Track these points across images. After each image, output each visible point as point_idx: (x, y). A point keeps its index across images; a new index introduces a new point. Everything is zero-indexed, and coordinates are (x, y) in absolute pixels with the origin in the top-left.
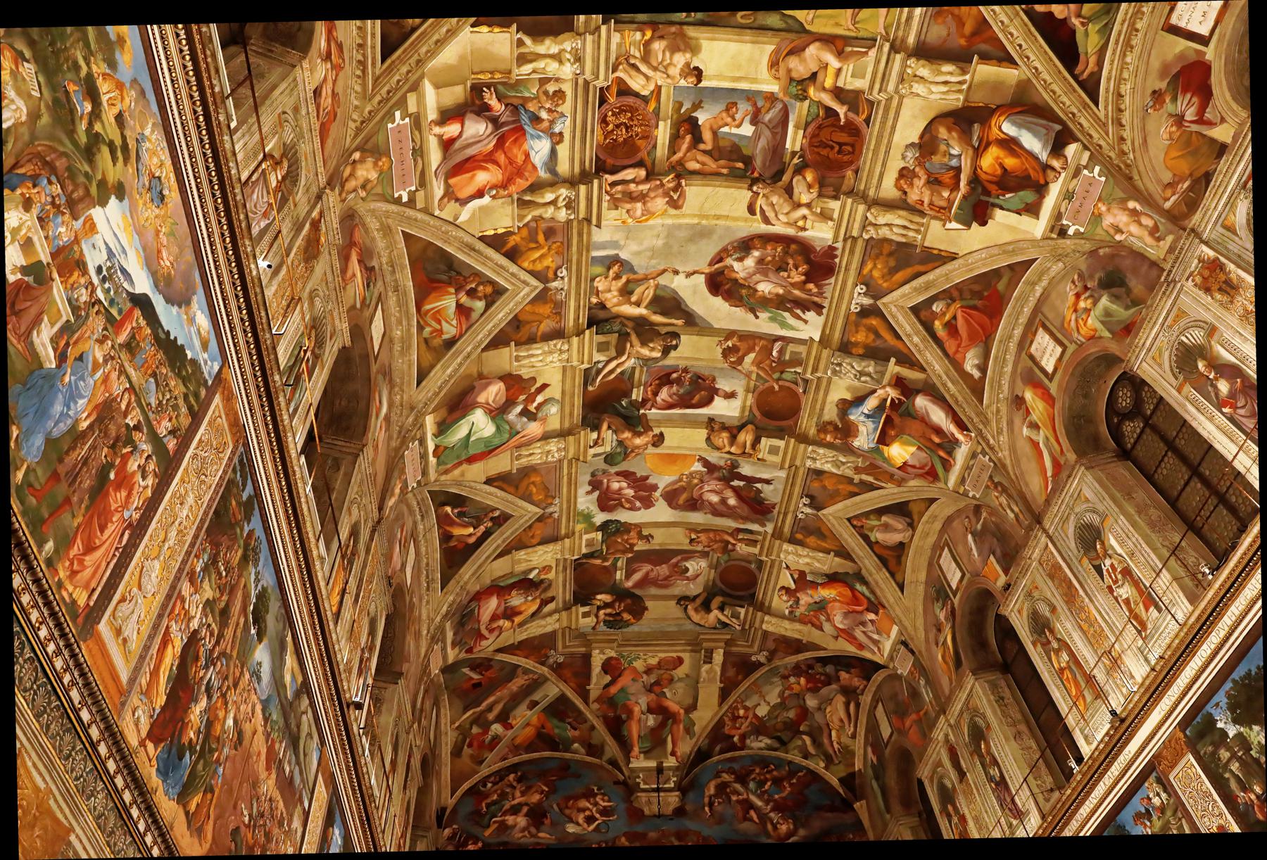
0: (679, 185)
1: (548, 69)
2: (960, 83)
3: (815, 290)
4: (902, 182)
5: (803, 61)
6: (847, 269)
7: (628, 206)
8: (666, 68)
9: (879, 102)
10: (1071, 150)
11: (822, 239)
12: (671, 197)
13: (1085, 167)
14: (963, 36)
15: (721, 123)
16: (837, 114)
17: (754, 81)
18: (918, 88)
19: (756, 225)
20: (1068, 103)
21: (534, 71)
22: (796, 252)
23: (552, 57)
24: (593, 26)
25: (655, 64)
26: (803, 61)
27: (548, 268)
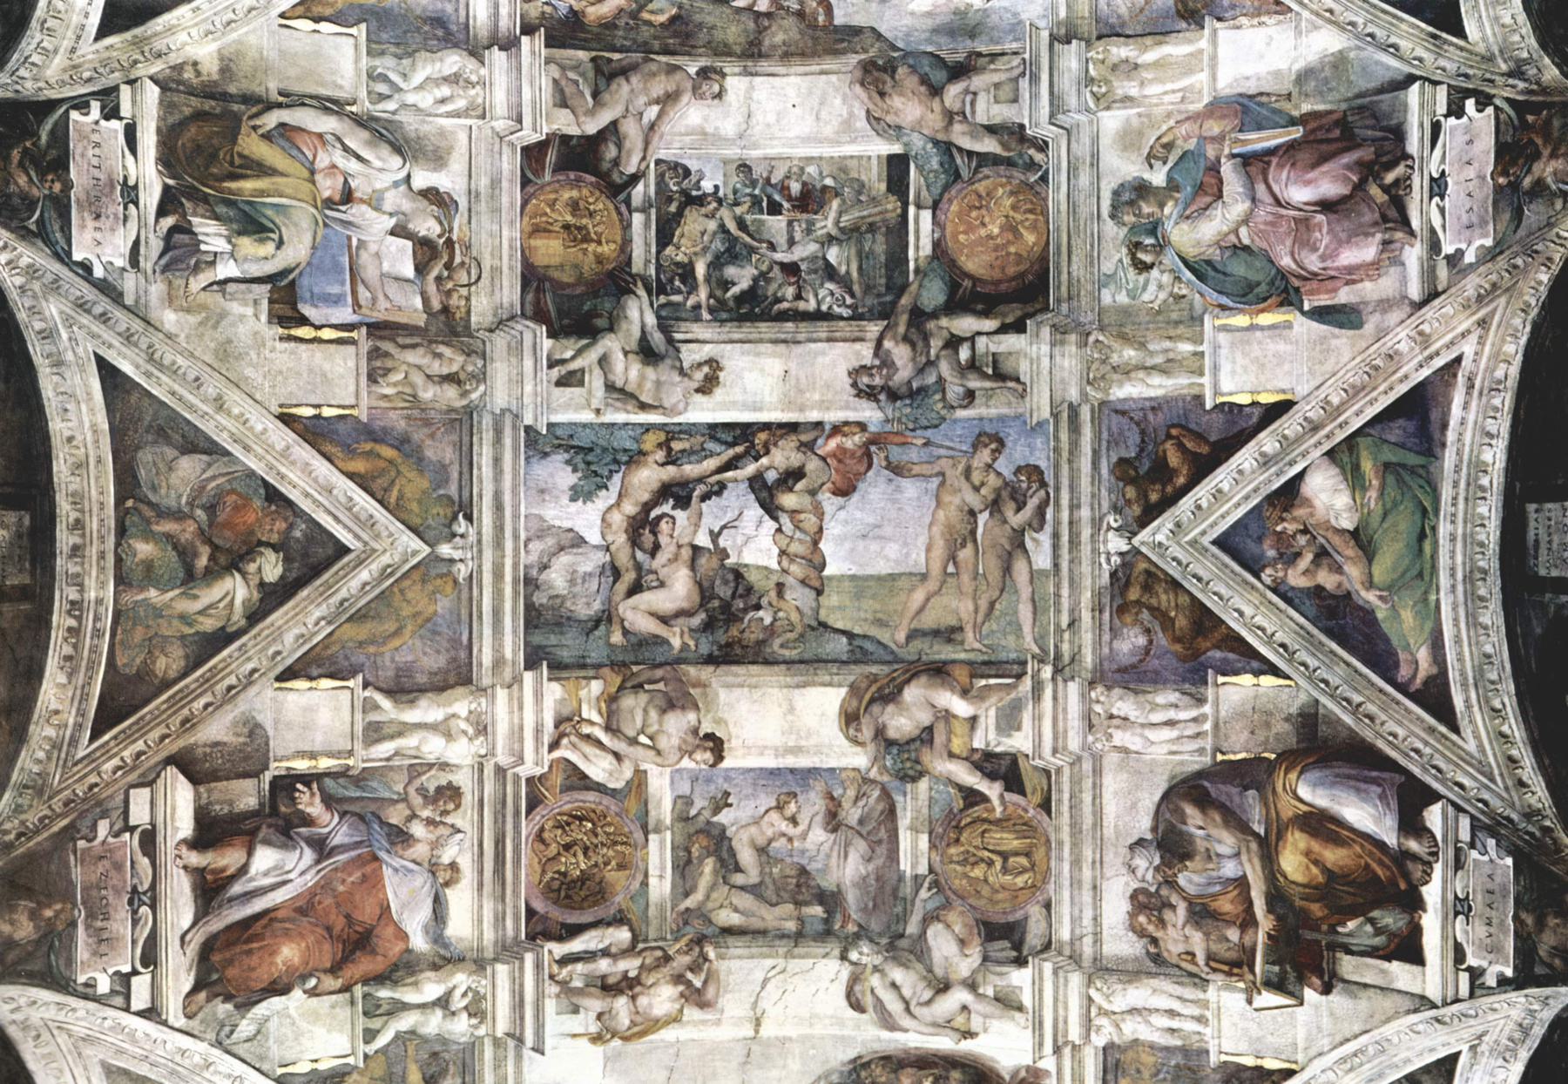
1: (425, 749)
2: (1195, 720)
9: (1059, 770)
10: (1434, 817)
12: (689, 984)
13: (1472, 845)
15: (770, 833)
16: (984, 799)
18: (1120, 738)
20: (1401, 732)
21: (397, 753)
24: (508, 674)
25: (631, 733)
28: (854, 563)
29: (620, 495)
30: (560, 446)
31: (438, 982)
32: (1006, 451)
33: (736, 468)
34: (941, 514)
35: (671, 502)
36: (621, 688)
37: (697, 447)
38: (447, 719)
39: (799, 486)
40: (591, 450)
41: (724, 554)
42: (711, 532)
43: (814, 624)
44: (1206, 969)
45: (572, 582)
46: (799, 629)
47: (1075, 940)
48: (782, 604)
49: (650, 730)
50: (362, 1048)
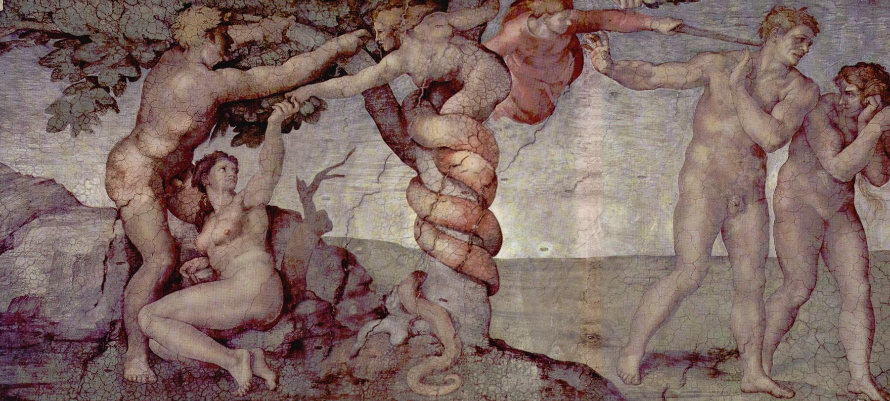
28: (549, 238)
29: (139, 119)
30: (28, 33)
32: (820, 41)
33: (343, 73)
34: (702, 154)
35: (231, 133)
37: (276, 37)
39: (453, 104)
40: (86, 40)
41: (323, 222)
42: (300, 185)
43: (484, 344)
45: (54, 273)
46: (451, 352)
48: (423, 309)
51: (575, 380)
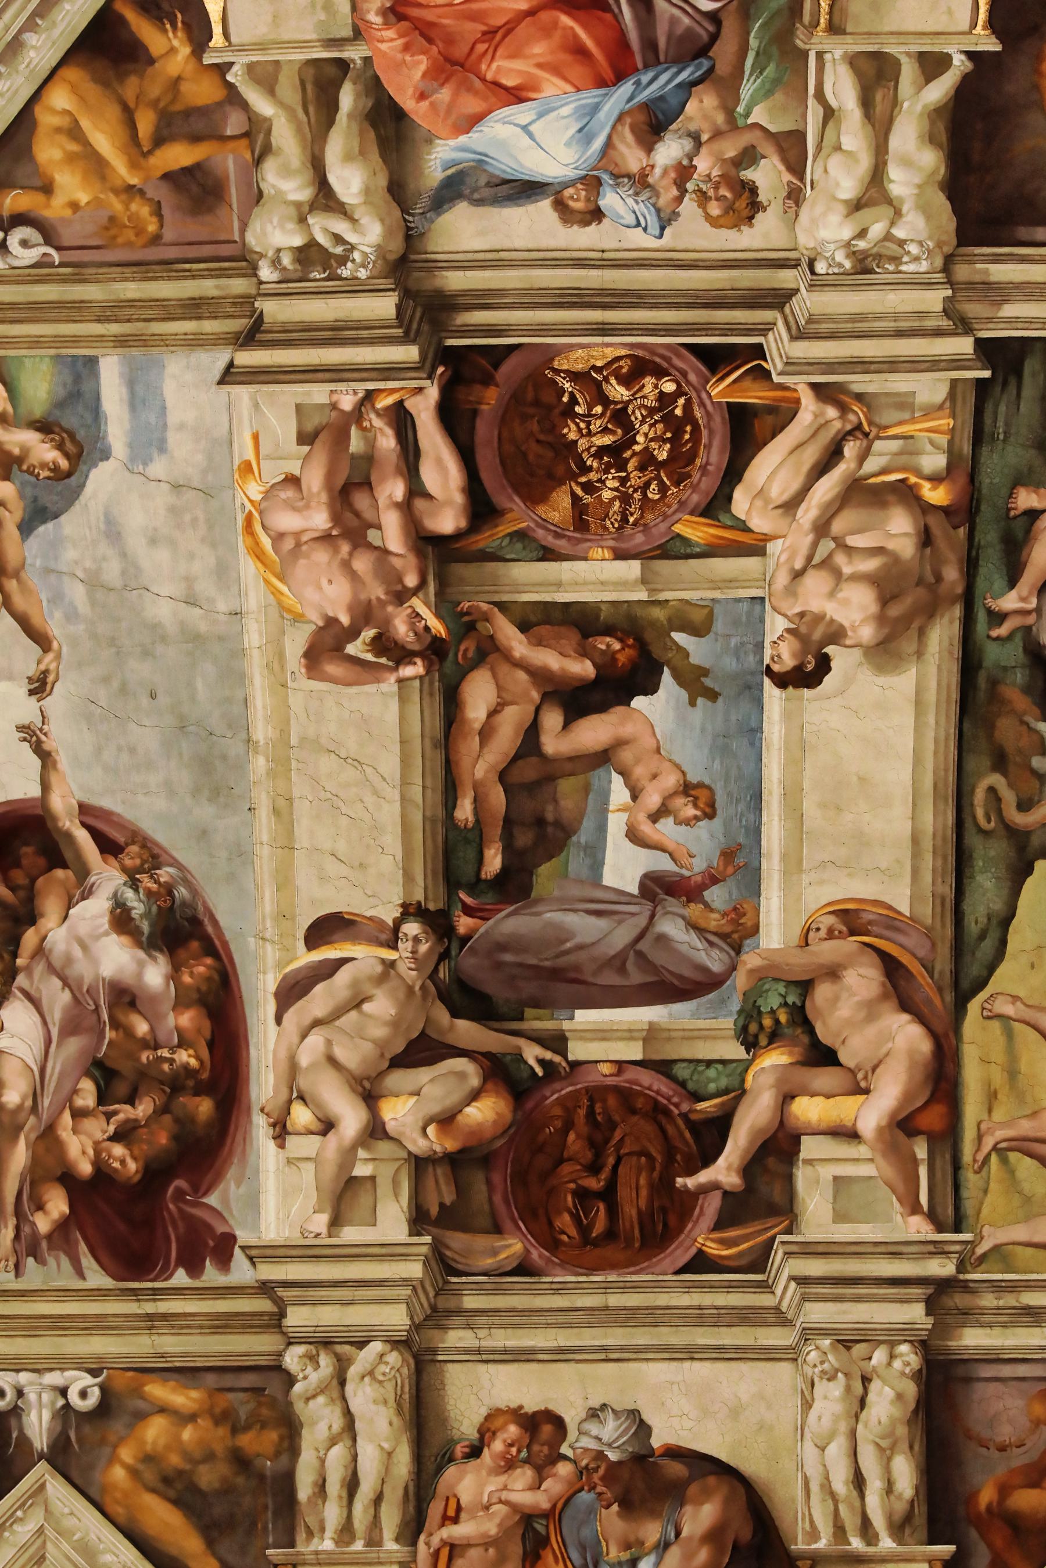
0: (400, 655)
1: (835, 163)
2: (866, 1527)
3: (43, 1224)
4: (513, 1430)
5: (870, 1011)
6: (151, 1322)
7: (315, 480)
8: (826, 563)
9: (766, 1287)
11: (253, 1203)
12: (353, 633)
14: (1004, 1490)
15: (639, 772)
16: (709, 1157)
17: (793, 864)
19: (271, 953)
21: (829, 114)
22: (184, 1123)
23: (877, 175)
24: (973, 309)
25: (837, 526)
26: (870, 1011)
27: (47, 189)
31: (367, 191)
36: (926, 508)
38: (889, 201)
44: (435, 1541)
46: (1021, 820)
47: (470, 1318)
49: (840, 559)
50: (241, 61)
51: (988, 946)
